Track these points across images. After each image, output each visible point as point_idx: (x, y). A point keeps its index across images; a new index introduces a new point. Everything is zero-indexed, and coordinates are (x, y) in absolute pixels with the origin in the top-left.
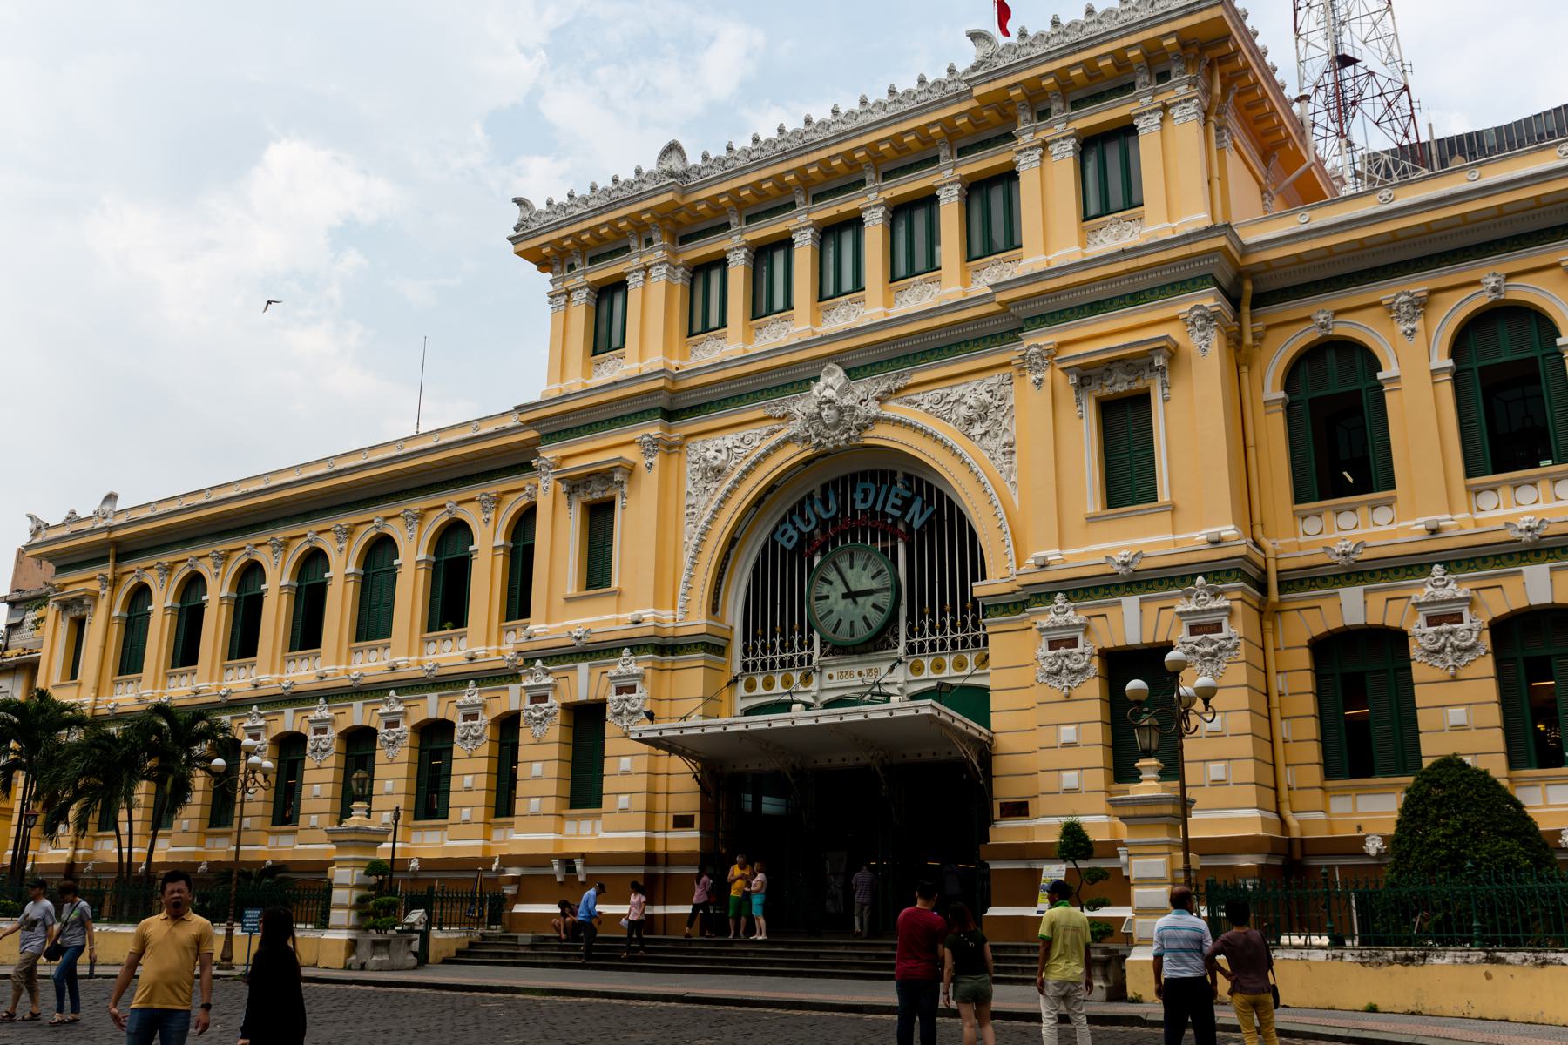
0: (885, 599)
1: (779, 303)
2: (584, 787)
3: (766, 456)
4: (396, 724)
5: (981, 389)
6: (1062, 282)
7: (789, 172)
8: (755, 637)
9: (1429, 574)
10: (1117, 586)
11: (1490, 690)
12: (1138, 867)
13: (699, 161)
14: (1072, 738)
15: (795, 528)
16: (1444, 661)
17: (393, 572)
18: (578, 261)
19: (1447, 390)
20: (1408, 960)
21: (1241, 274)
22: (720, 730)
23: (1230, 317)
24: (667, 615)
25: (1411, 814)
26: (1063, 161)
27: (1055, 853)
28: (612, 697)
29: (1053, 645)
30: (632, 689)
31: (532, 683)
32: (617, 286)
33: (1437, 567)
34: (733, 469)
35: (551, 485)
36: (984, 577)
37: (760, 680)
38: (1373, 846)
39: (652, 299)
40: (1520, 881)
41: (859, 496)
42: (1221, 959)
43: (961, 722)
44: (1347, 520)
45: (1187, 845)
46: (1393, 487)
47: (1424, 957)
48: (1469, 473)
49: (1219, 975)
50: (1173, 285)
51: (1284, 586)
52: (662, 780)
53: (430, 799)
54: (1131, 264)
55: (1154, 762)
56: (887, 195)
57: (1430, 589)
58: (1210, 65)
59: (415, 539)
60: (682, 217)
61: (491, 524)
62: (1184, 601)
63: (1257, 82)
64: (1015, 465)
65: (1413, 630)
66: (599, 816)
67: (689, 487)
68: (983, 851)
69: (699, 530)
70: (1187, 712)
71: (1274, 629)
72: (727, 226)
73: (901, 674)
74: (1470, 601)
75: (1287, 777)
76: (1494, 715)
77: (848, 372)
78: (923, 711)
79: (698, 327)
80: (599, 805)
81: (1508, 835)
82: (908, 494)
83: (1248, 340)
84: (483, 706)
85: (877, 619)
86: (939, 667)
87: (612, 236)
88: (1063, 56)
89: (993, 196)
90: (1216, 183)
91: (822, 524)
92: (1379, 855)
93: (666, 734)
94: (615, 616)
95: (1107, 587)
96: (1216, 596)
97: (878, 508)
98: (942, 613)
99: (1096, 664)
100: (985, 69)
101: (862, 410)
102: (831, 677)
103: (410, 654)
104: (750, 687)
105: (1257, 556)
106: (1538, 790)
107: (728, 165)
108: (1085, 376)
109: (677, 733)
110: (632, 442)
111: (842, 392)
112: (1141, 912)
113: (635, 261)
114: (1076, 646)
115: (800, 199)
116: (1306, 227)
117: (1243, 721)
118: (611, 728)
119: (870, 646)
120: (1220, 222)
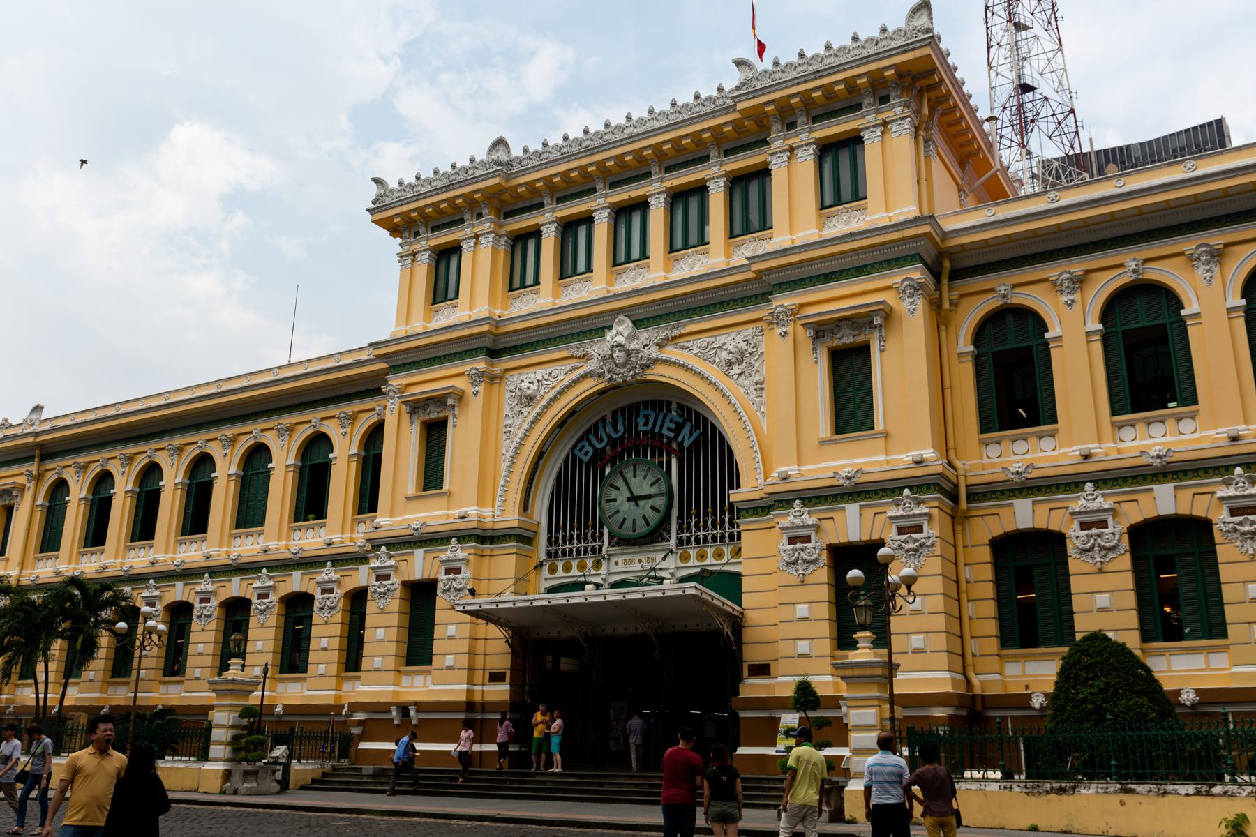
0: (660, 502)
1: (581, 266)
2: (417, 650)
3: (568, 387)
4: (267, 596)
5: (738, 339)
6: (803, 256)
7: (591, 164)
8: (557, 531)
9: (1082, 490)
10: (842, 495)
11: (1128, 580)
12: (854, 716)
13: (520, 154)
14: (806, 615)
15: (590, 445)
16: (1093, 558)
17: (267, 474)
18: (422, 229)
19: (1098, 348)
20: (1062, 791)
21: (942, 254)
22: (528, 604)
23: (932, 287)
24: (487, 512)
25: (1066, 676)
26: (806, 162)
27: (790, 705)
28: (442, 576)
29: (792, 541)
30: (458, 571)
31: (378, 564)
32: (454, 249)
33: (1088, 484)
34: (542, 397)
35: (397, 407)
36: (739, 486)
37: (560, 565)
38: (1037, 701)
39: (481, 261)
40: (1148, 729)
41: (641, 420)
42: (916, 789)
43: (719, 600)
44: (1020, 447)
45: (893, 700)
46: (1056, 422)
47: (1074, 788)
48: (1114, 413)
49: (915, 803)
50: (888, 262)
51: (971, 497)
52: (481, 643)
53: (293, 656)
54: (857, 244)
55: (868, 634)
56: (668, 184)
57: (1083, 501)
58: (920, 92)
59: (285, 447)
60: (506, 197)
61: (348, 437)
62: (894, 507)
63: (956, 106)
64: (764, 399)
65: (1069, 533)
66: (429, 672)
67: (507, 410)
68: (734, 703)
69: (514, 445)
70: (894, 595)
71: (963, 532)
72: (542, 205)
73: (672, 562)
74: (1113, 511)
75: (972, 646)
76: (1130, 600)
77: (634, 323)
78: (689, 592)
79: (517, 284)
80: (429, 663)
81: (1140, 693)
82: (680, 420)
83: (946, 305)
84: (338, 582)
85: (654, 518)
86: (702, 557)
87: (450, 211)
88: (806, 81)
89: (750, 187)
90: (924, 183)
91: (612, 442)
92: (1042, 708)
93: (484, 607)
94: (445, 512)
95: (834, 496)
96: (918, 505)
97: (656, 430)
98: (706, 514)
99: (824, 557)
100: (746, 89)
101: (645, 353)
102: (617, 563)
103: (279, 539)
104: (553, 570)
105: (950, 474)
106: (1163, 659)
107: (544, 157)
108: (820, 330)
109: (494, 606)
110: (462, 374)
111: (630, 338)
112: (856, 752)
113: (468, 230)
114: (809, 541)
115: (599, 186)
116: (992, 219)
117: (938, 603)
118: (441, 601)
119: (648, 540)
120: (926, 214)
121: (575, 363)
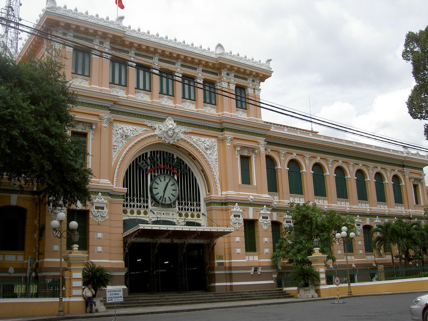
121: (148, 129)
